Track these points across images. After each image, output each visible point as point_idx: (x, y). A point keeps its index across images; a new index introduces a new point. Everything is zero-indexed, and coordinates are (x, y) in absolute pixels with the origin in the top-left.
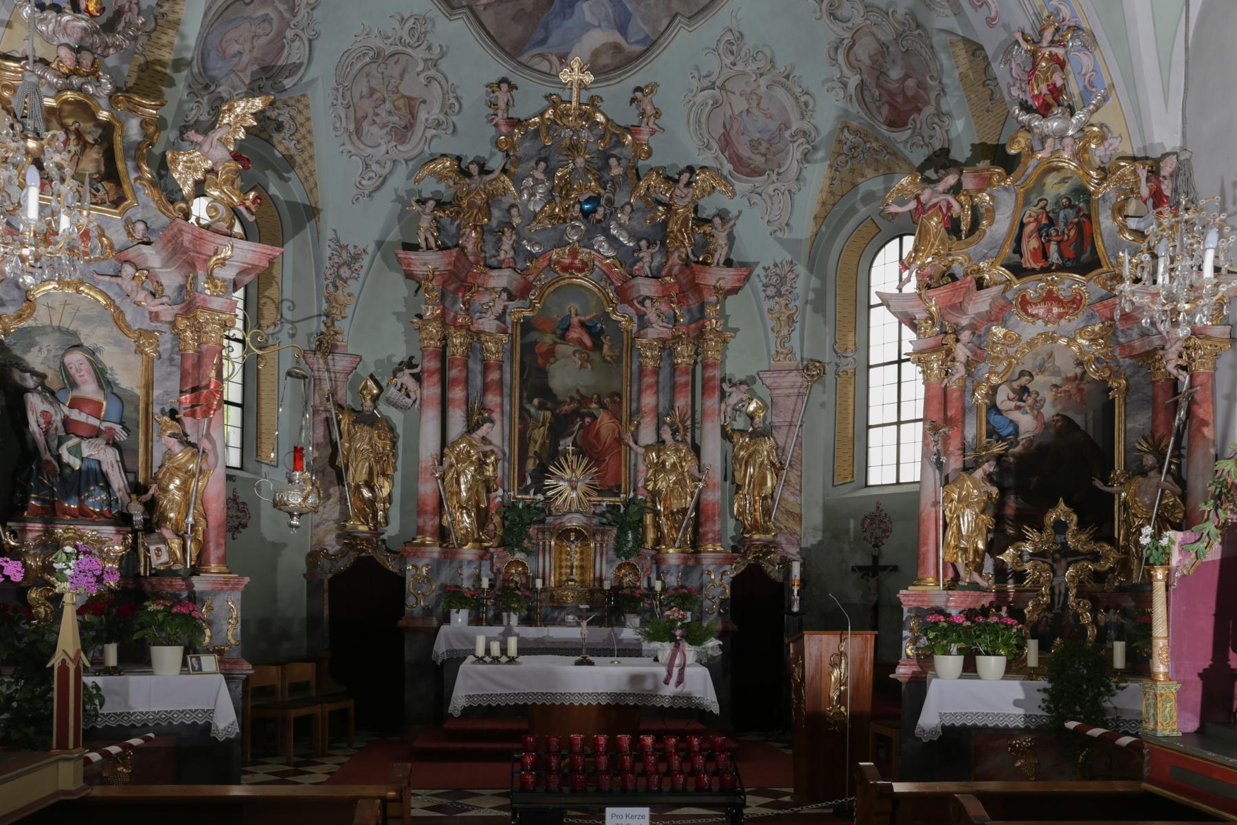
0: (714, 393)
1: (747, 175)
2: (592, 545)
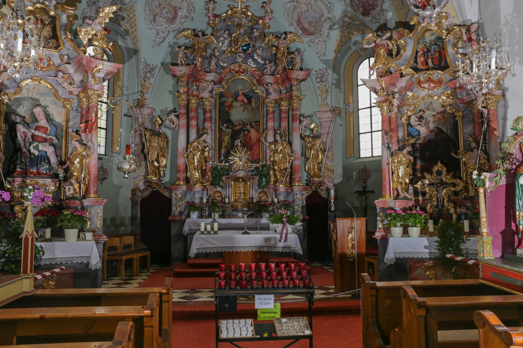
0: (297, 121)
1: (308, 35)
2: (249, 184)
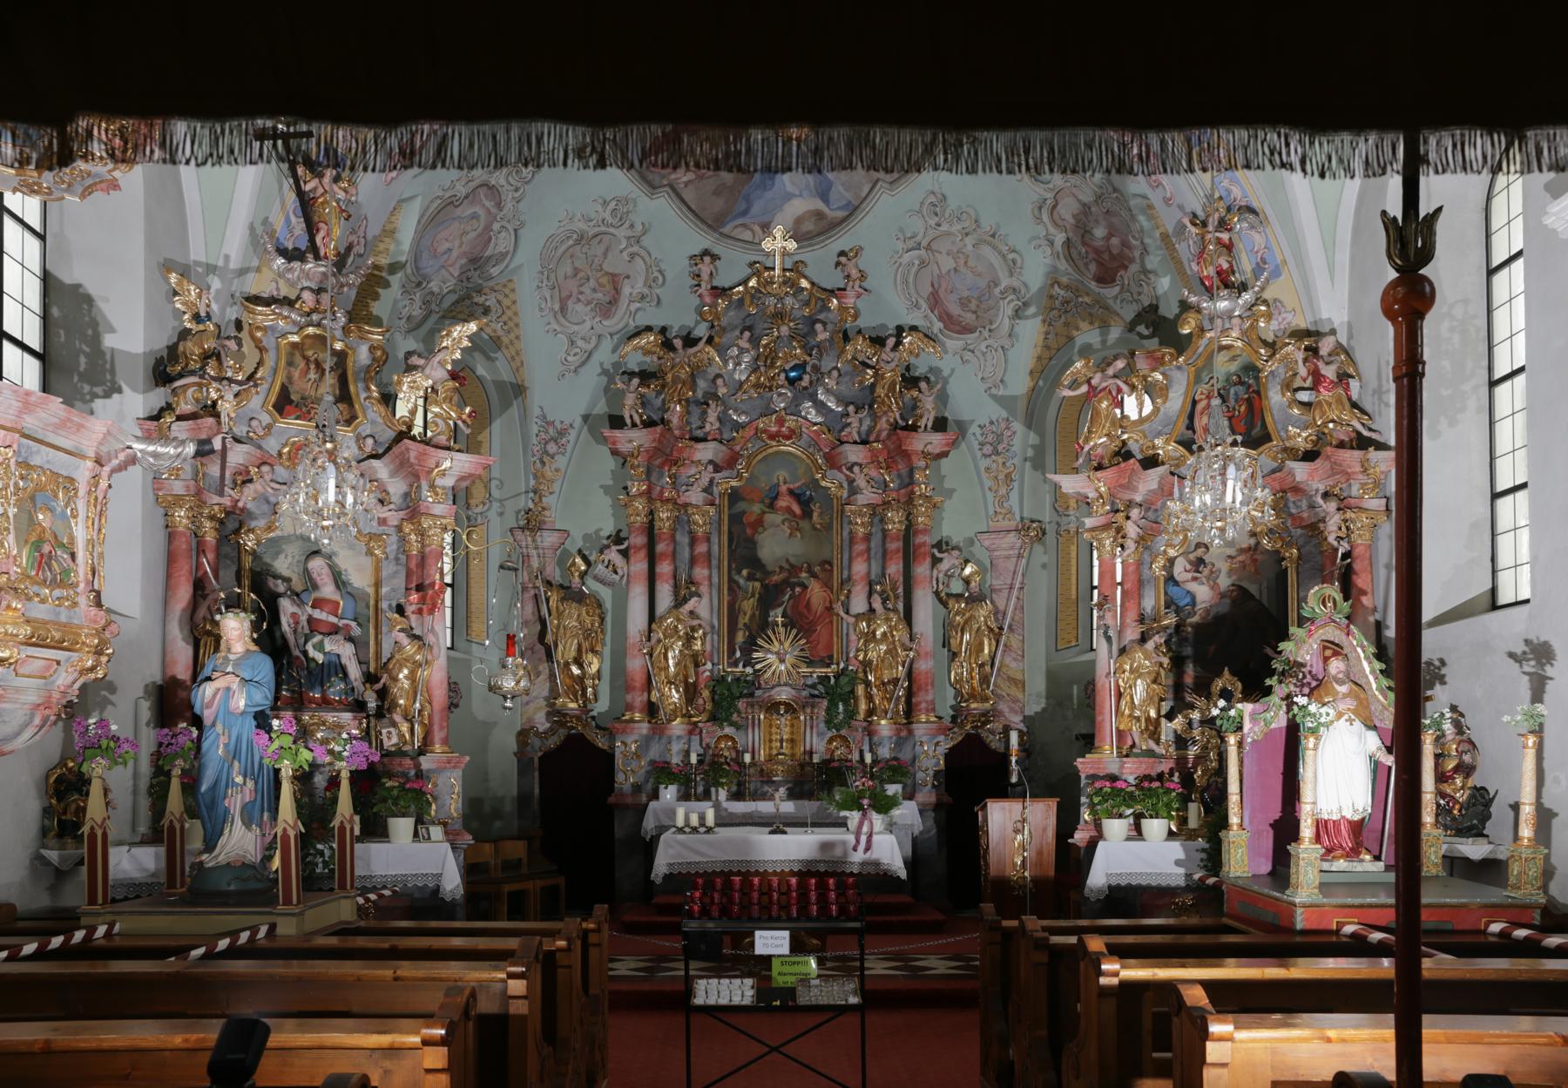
1: (959, 332)
